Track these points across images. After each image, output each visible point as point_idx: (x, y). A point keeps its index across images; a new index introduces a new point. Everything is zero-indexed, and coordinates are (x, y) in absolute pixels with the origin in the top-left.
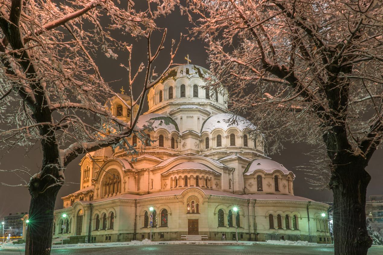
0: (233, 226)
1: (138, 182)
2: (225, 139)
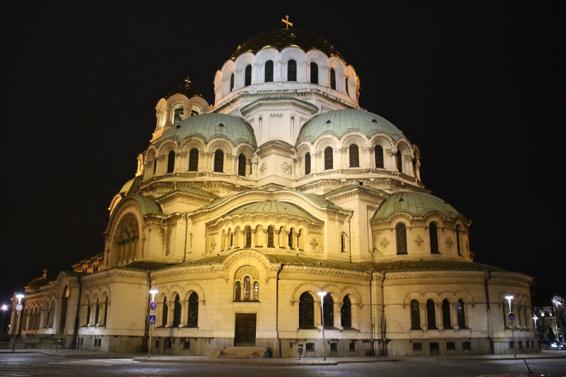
0: (335, 325)
1: (166, 237)
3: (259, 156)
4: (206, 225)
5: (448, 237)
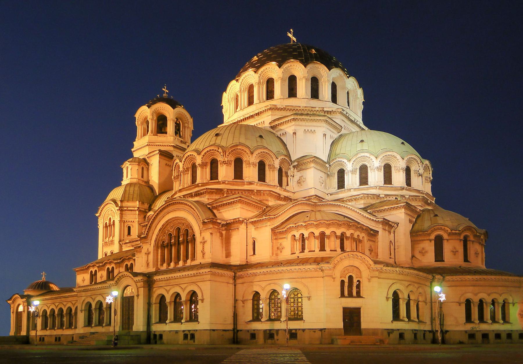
1: (227, 242)
2: (376, 171)
3: (295, 169)
5: (476, 248)
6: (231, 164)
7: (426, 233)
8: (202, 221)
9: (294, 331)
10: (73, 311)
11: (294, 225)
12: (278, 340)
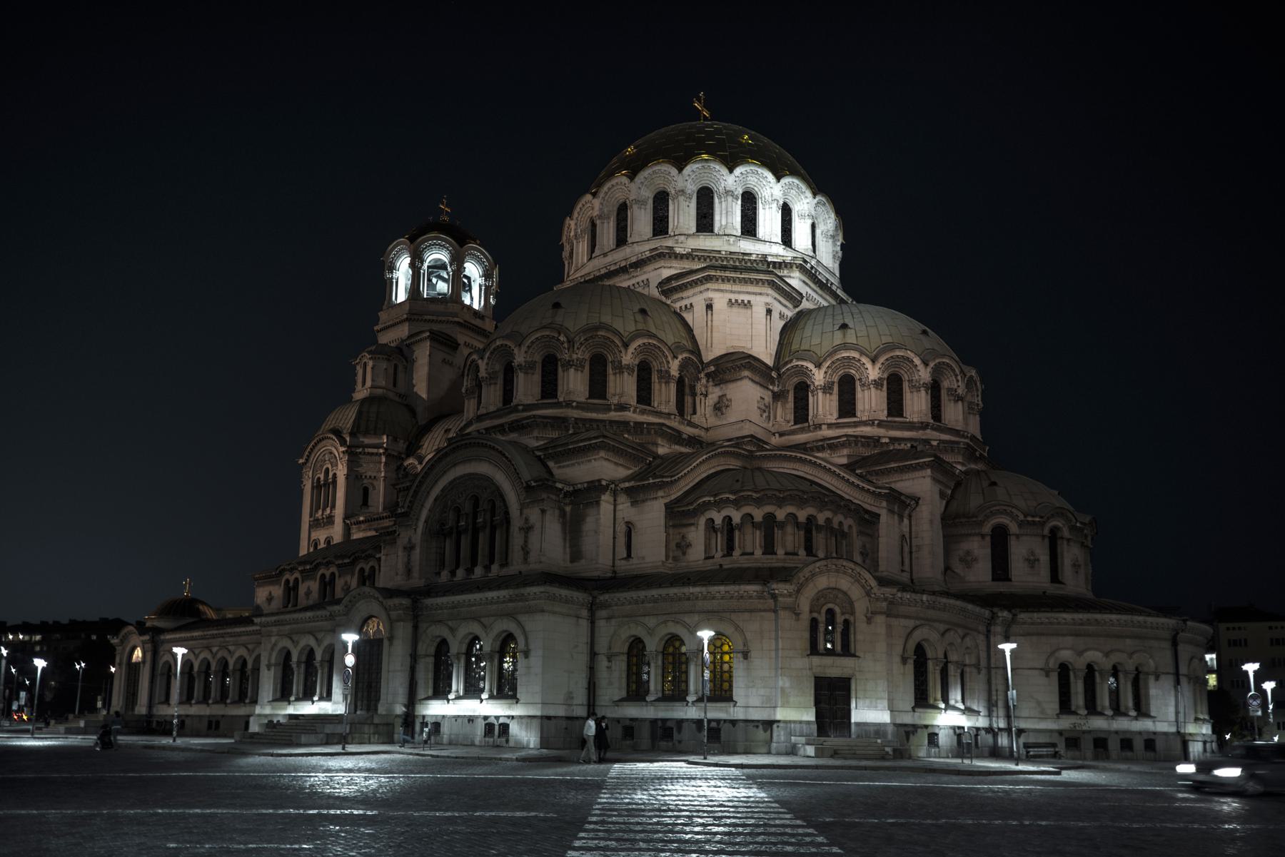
1: (573, 530)
4: (666, 509)
6: (583, 367)
7: (974, 519)
8: (525, 485)
9: (714, 725)
10: (250, 666)
11: (712, 499)
12: (680, 742)
